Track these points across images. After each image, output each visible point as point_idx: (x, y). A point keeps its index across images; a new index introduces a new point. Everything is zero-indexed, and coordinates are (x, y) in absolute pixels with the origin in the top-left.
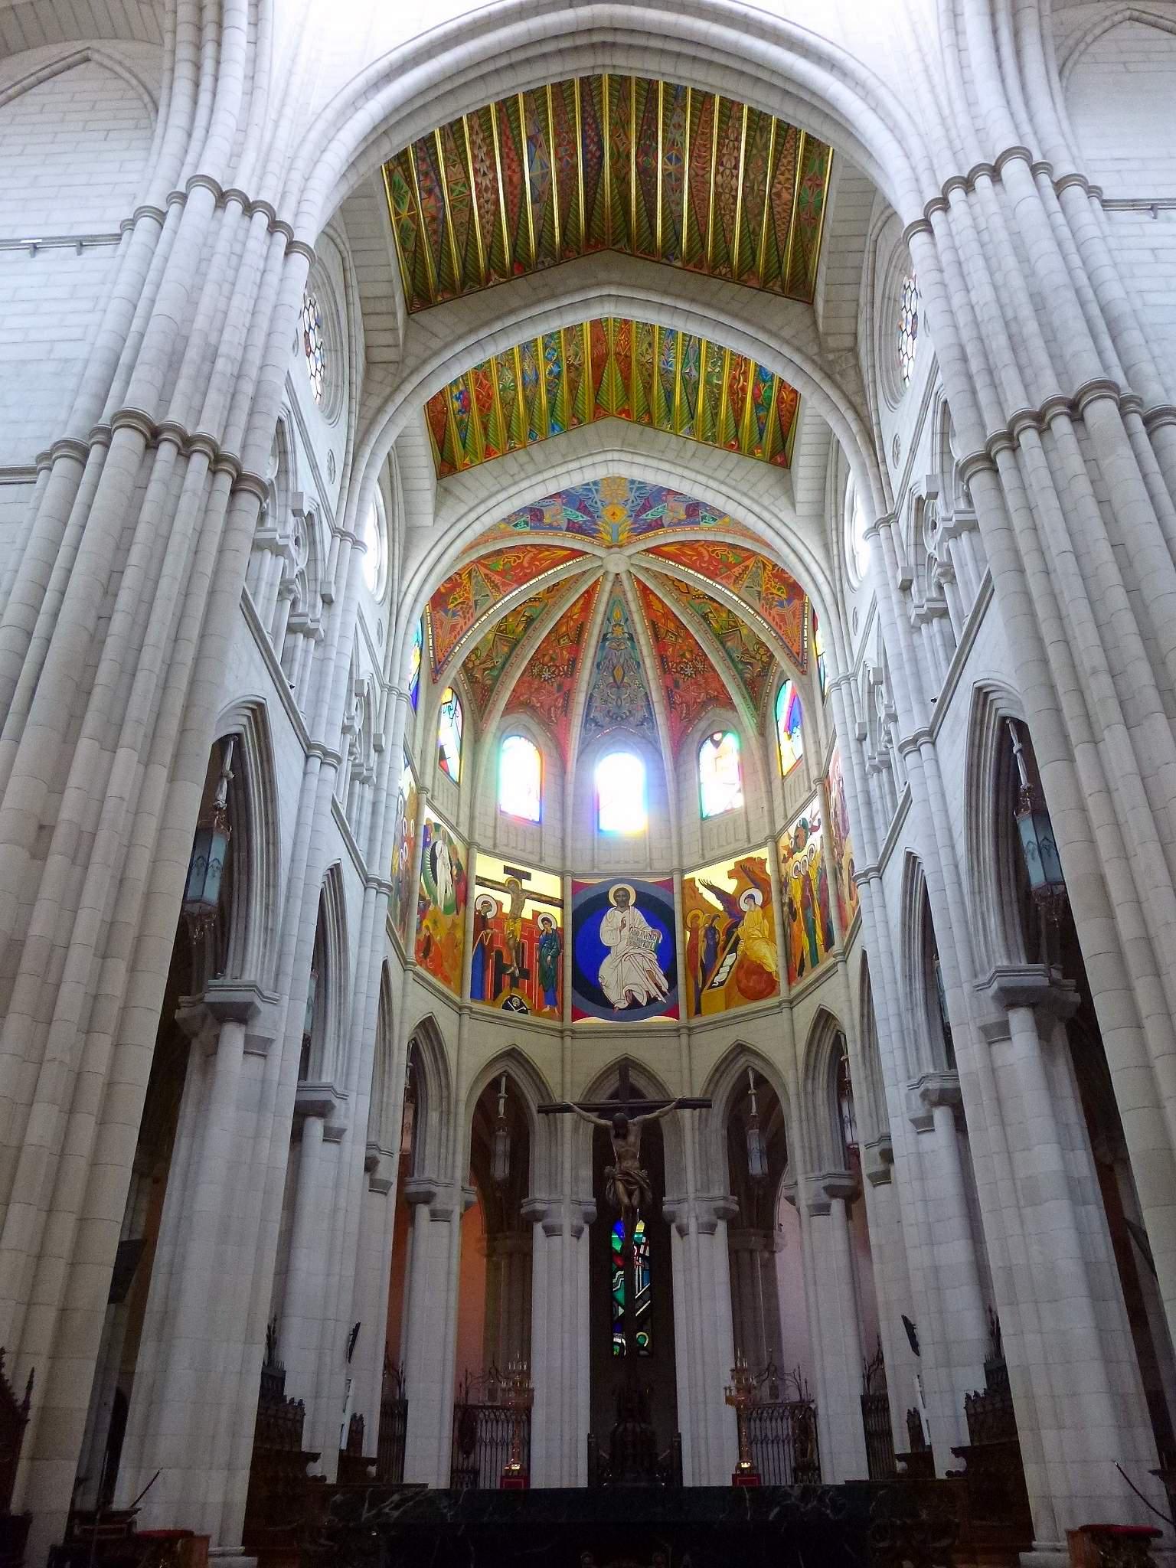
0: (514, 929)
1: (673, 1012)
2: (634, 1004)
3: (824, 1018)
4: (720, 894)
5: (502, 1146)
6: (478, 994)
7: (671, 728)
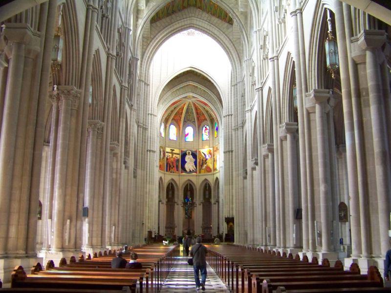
0: (172, 159)
1: (196, 172)
2: (190, 171)
3: (217, 178)
4: (204, 154)
5: (170, 193)
6: (167, 171)
7: (198, 124)
